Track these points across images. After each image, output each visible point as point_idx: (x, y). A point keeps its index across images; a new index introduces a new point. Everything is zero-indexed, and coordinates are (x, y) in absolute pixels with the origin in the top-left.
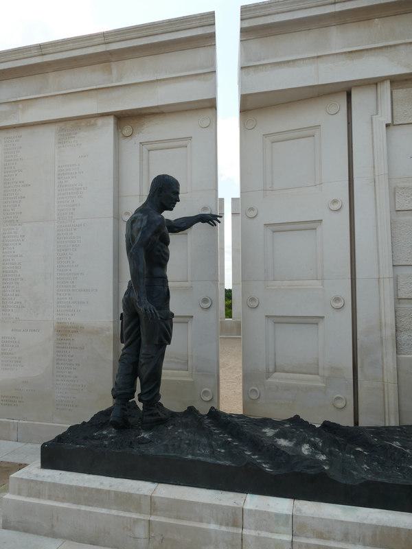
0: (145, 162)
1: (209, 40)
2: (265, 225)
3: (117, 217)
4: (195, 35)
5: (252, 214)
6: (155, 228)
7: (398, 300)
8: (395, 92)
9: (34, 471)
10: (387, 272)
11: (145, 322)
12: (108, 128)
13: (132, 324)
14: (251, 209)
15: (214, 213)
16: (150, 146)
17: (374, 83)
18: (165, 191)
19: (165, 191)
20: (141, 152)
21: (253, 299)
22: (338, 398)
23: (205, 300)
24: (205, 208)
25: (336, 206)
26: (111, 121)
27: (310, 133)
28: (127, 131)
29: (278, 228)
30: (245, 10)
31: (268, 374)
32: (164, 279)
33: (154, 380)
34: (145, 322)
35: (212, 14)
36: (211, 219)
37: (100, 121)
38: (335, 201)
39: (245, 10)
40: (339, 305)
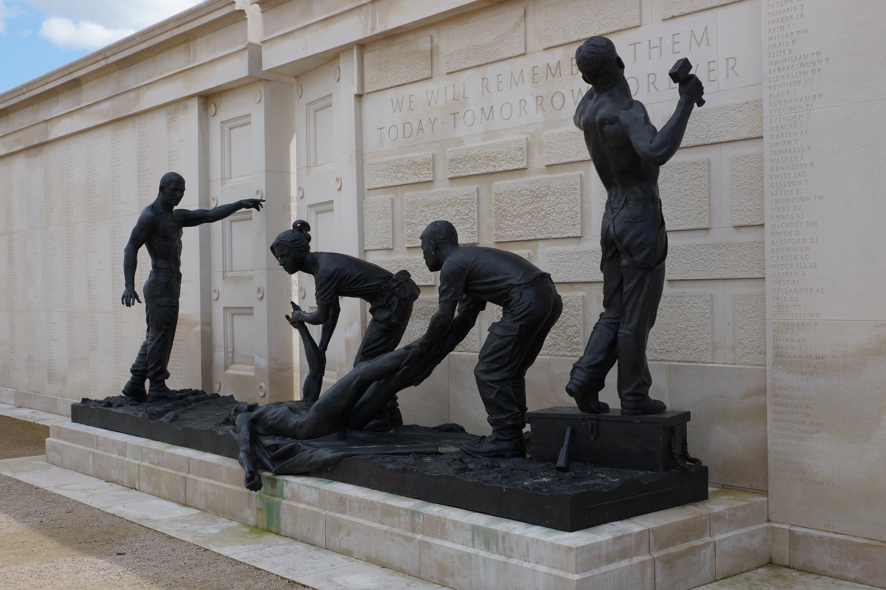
0: (226, 142)
2: (310, 206)
9: (67, 424)
20: (222, 132)
28: (212, 110)
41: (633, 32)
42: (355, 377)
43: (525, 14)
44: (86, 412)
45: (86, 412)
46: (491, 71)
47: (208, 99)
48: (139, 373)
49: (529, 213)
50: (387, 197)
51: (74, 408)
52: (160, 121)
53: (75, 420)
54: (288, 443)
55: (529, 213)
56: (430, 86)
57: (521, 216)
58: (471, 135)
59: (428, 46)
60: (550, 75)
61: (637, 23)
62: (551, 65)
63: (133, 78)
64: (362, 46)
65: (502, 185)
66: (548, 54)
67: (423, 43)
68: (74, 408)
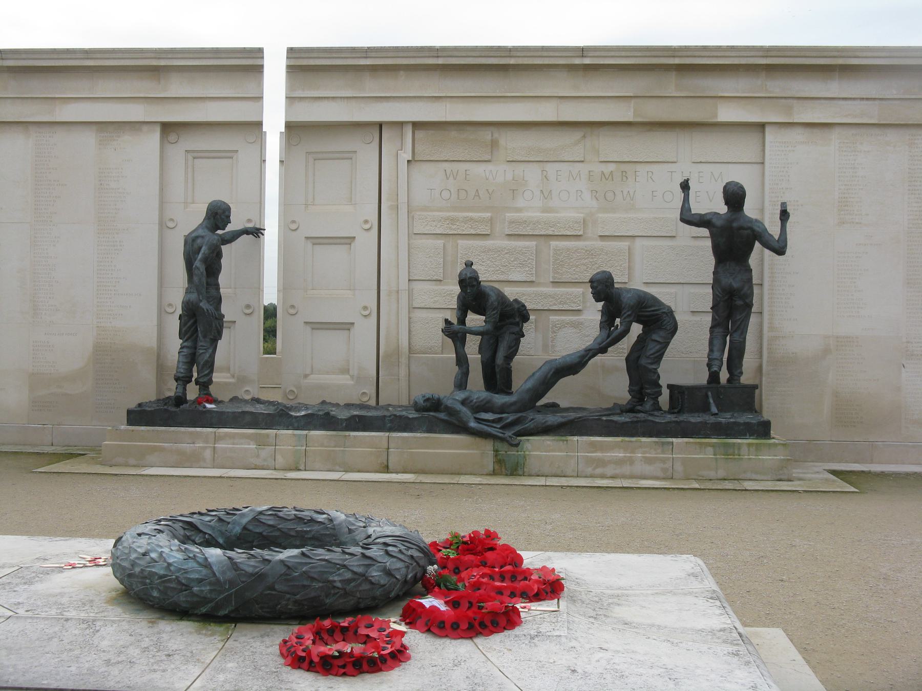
1: (258, 70)
3: (164, 226)
4: (245, 65)
5: (294, 226)
6: (211, 245)
7: (412, 308)
8: (416, 132)
10: (404, 284)
11: (201, 322)
12: (154, 138)
13: (192, 321)
14: (294, 222)
15: (258, 226)
16: (195, 155)
17: (401, 124)
18: (218, 215)
19: (218, 215)
21: (293, 307)
22: (364, 393)
23: (248, 306)
24: (249, 221)
25: (367, 226)
26: (158, 129)
27: (349, 156)
28: (172, 137)
29: (317, 241)
30: (291, 51)
31: (306, 376)
32: (218, 285)
33: (209, 365)
34: (201, 322)
35: (260, 51)
36: (257, 232)
37: (145, 128)
38: (366, 222)
39: (291, 51)
40: (367, 313)
41: (670, 165)
42: (550, 370)
43: (584, 137)
44: (139, 416)
45: (139, 416)
46: (551, 168)
47: (167, 128)
48: (183, 380)
49: (584, 265)
50: (440, 242)
51: (129, 412)
52: (89, 139)
53: (131, 422)
54: (511, 418)
55: (584, 265)
56: (489, 167)
57: (577, 266)
58: (530, 208)
59: (489, 137)
60: (604, 179)
61: (675, 160)
62: (605, 172)
63: (37, 87)
64: (416, 125)
65: (554, 243)
66: (603, 165)
67: (487, 135)
68: (129, 412)
